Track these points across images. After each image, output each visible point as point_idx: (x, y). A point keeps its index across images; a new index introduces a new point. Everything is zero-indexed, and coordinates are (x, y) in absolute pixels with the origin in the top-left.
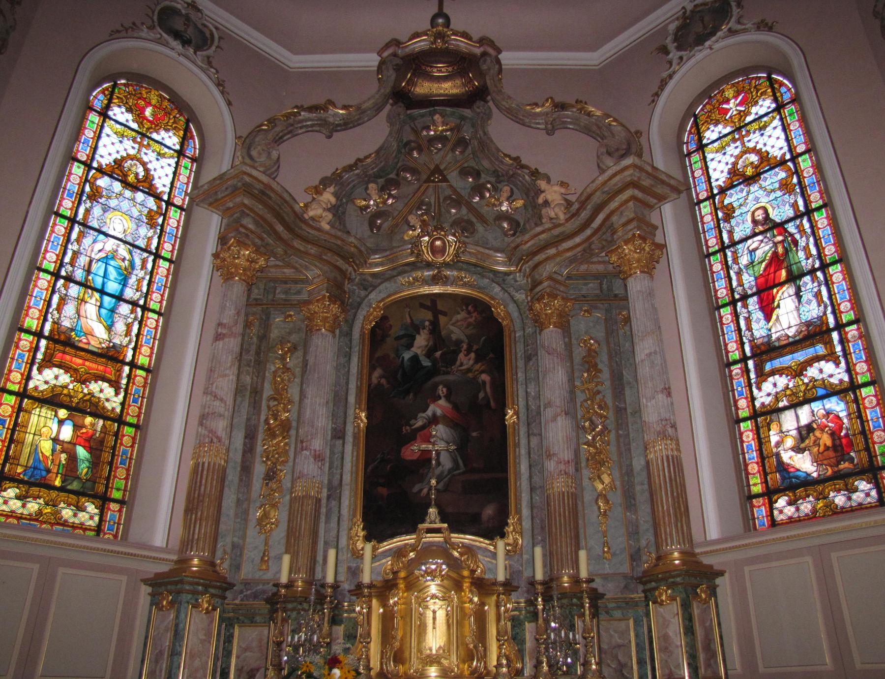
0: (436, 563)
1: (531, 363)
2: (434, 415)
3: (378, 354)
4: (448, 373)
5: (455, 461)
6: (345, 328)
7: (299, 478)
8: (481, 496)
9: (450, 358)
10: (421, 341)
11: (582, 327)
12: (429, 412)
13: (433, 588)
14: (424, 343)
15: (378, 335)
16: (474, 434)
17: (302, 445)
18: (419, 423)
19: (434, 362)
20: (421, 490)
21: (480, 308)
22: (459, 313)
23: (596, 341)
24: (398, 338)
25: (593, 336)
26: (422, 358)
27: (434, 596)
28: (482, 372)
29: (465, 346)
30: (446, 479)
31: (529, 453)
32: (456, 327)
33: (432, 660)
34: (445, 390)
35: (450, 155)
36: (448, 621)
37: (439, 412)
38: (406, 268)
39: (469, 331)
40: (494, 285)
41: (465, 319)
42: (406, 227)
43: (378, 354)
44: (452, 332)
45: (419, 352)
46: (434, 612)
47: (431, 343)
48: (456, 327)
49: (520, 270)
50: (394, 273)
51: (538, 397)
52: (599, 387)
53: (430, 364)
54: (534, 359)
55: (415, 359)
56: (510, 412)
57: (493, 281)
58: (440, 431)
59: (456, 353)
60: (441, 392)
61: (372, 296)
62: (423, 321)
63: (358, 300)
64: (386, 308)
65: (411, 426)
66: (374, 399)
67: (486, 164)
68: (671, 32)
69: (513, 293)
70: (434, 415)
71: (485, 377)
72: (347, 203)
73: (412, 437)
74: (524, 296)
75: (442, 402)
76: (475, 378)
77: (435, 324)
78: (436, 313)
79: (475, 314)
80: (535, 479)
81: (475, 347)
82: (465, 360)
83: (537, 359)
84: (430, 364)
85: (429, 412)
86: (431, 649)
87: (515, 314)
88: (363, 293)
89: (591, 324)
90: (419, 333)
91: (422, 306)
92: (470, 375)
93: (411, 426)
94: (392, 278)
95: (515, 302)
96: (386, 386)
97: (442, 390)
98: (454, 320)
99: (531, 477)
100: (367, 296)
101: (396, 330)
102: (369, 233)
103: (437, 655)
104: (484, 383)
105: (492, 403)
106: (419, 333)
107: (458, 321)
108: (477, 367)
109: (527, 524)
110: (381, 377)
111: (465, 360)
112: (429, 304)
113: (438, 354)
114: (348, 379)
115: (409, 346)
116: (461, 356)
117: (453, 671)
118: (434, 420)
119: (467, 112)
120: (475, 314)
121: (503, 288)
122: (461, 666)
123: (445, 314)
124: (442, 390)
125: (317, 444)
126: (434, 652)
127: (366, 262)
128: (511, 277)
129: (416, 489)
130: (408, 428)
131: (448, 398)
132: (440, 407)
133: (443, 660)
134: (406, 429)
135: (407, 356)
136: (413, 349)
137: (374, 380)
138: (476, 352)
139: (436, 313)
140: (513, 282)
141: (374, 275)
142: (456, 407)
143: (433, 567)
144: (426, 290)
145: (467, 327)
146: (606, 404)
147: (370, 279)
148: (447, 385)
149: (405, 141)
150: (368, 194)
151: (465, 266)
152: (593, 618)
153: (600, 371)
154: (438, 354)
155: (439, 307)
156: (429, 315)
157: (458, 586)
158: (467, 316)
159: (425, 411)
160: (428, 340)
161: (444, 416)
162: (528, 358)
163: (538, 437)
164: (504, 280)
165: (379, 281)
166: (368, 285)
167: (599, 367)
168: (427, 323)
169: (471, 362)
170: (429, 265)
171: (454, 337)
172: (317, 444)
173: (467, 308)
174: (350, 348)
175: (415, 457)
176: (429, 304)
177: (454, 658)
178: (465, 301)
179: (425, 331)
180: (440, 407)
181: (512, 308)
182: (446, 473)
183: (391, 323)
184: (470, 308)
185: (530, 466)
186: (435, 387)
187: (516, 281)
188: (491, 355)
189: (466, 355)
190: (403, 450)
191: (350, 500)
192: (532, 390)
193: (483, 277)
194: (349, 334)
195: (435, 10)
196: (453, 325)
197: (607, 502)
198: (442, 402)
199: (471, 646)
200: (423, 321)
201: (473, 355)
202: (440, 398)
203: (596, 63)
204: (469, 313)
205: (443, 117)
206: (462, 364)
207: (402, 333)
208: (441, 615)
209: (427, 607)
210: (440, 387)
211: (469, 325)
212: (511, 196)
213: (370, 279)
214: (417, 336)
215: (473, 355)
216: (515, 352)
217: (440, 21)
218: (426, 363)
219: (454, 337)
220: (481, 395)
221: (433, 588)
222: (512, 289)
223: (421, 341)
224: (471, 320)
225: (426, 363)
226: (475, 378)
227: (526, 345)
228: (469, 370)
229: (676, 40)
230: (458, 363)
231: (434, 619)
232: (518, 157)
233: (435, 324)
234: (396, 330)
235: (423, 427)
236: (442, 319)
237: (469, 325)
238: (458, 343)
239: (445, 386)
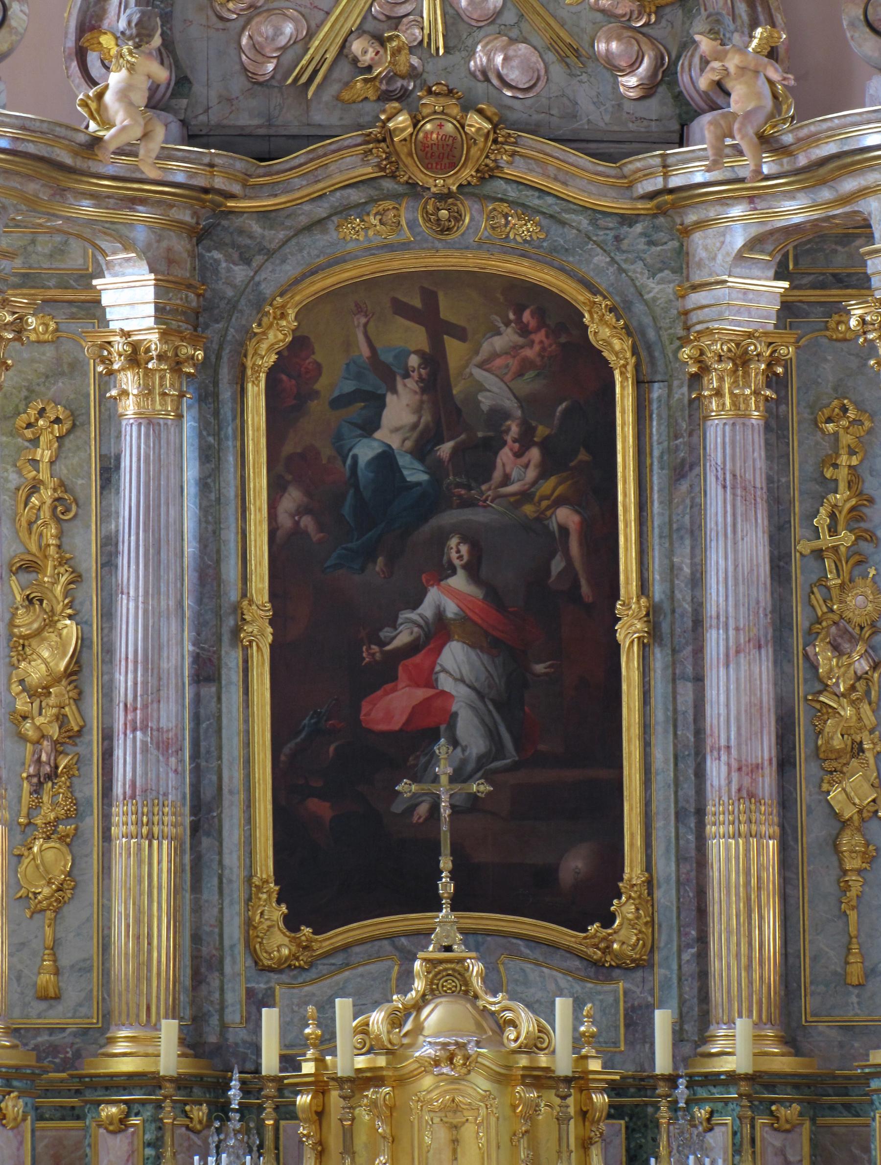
2: (440, 615)
3: (288, 448)
5: (492, 735)
9: (478, 458)
10: (400, 411)
12: (427, 609)
16: (540, 668)
18: (403, 638)
19: (436, 470)
22: (499, 333)
28: (559, 502)
29: (514, 429)
34: (464, 549)
37: (451, 609)
43: (288, 448)
44: (482, 388)
45: (395, 442)
47: (426, 418)
48: (491, 370)
55: (386, 458)
58: (455, 656)
59: (493, 445)
60: (454, 555)
62: (403, 355)
65: (382, 644)
70: (440, 615)
71: (565, 516)
73: (385, 673)
75: (459, 582)
76: (541, 519)
78: (438, 329)
79: (540, 336)
81: (542, 431)
82: (517, 468)
91: (402, 309)
92: (529, 509)
93: (382, 644)
96: (315, 536)
97: (457, 550)
101: (332, 380)
104: (564, 530)
105: (585, 589)
108: (547, 486)
110: (301, 511)
111: (517, 468)
112: (417, 303)
113: (445, 449)
115: (370, 426)
116: (505, 455)
118: (438, 632)
123: (461, 334)
124: (457, 550)
130: (375, 648)
131: (473, 570)
132: (453, 593)
134: (370, 653)
135: (365, 452)
137: (285, 521)
138: (545, 446)
139: (438, 329)
142: (493, 594)
145: (520, 374)
154: (445, 449)
155: (447, 311)
160: (418, 410)
161: (464, 620)
168: (414, 361)
169: (531, 474)
175: (396, 724)
176: (417, 303)
179: (411, 383)
180: (453, 593)
186: (440, 540)
188: (583, 456)
190: (365, 707)
198: (459, 582)
201: (535, 454)
204: (524, 331)
206: (506, 480)
207: (349, 386)
210: (453, 542)
211: (525, 366)
213: (256, 228)
214: (390, 398)
218: (415, 473)
219: (486, 401)
220: (557, 565)
223: (400, 411)
224: (529, 353)
226: (541, 519)
228: (525, 496)
230: (497, 475)
234: (332, 380)
235: (413, 648)
237: (525, 366)
238: (498, 416)
239: (464, 539)
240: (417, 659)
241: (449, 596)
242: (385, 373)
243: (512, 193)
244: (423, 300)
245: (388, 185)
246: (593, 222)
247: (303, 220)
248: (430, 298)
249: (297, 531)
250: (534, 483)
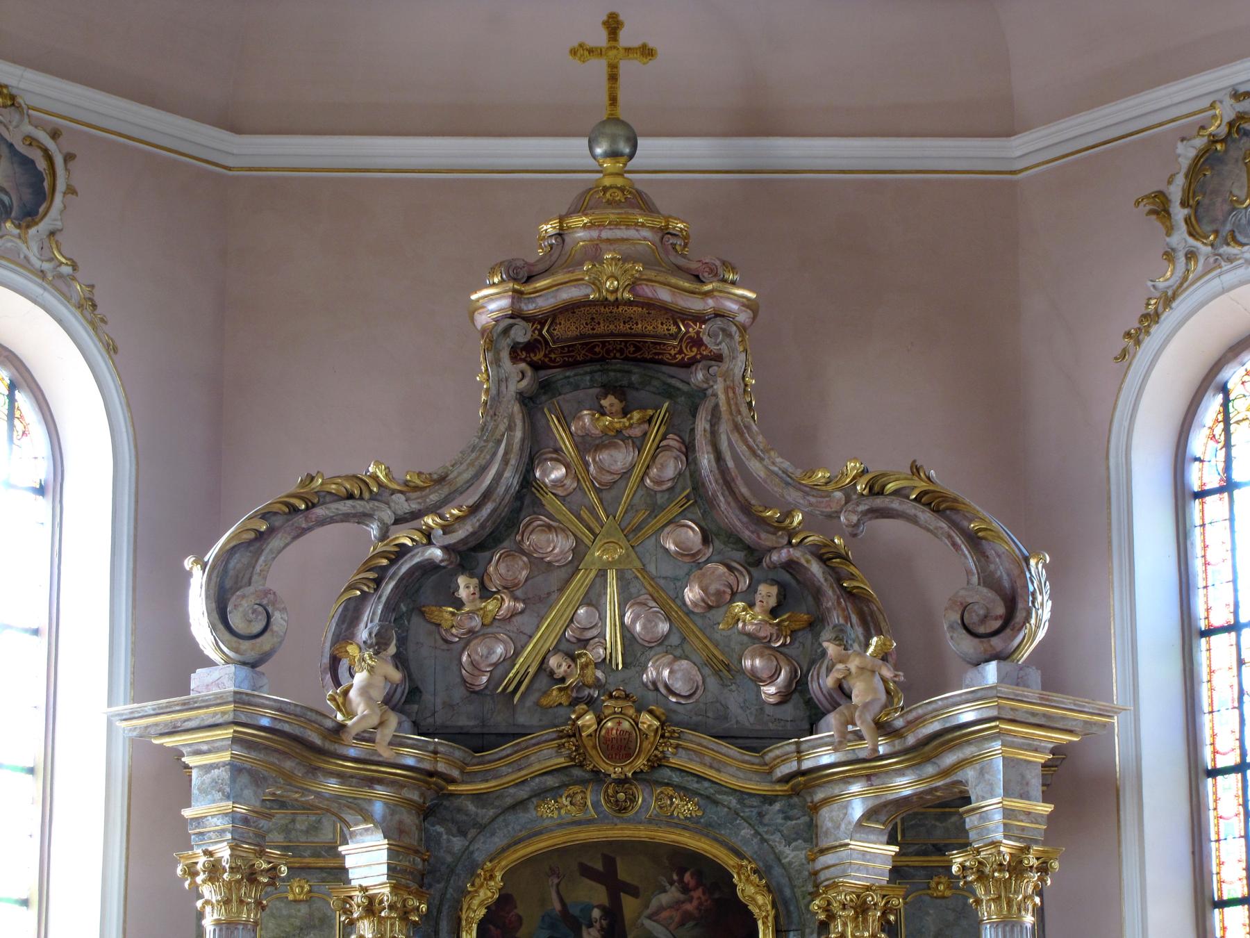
22: (665, 891)
38: (551, 781)
41: (676, 904)
62: (588, 909)
78: (617, 889)
79: (698, 893)
91: (587, 872)
98: (654, 903)
107: (661, 908)
112: (599, 866)
120: (698, 893)
123: (634, 892)
128: (777, 806)
139: (617, 889)
145: (682, 924)
151: (676, 778)
155: (623, 874)
156: (597, 894)
158: (682, 897)
164: (761, 815)
165: (491, 812)
168: (596, 913)
173: (681, 872)
176: (599, 866)
183: (520, 910)
184: (687, 877)
196: (650, 917)
200: (588, 909)
204: (685, 889)
211: (686, 917)
213: (471, 808)
222: (777, 837)
224: (688, 907)
236: (629, 904)
243: (676, 778)
244: (603, 865)
245: (577, 772)
246: (741, 801)
247: (509, 801)
248: (610, 862)
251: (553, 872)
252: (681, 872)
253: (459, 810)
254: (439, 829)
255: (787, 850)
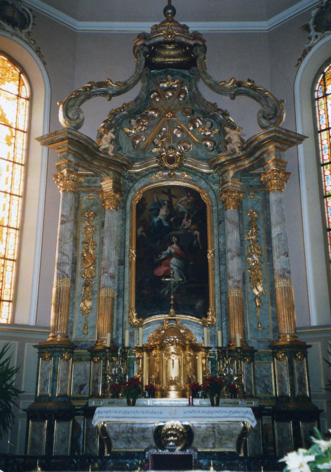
0: (174, 338)
1: (221, 226)
2: (171, 252)
3: (140, 219)
4: (177, 230)
6: (122, 204)
7: (103, 288)
8: (194, 296)
9: (179, 221)
10: (163, 212)
11: (250, 204)
12: (168, 251)
13: (172, 349)
14: (164, 213)
15: (141, 207)
16: (191, 263)
17: (105, 270)
18: (163, 257)
19: (170, 223)
20: (164, 293)
21: (194, 194)
22: (183, 197)
23: (257, 213)
24: (151, 210)
25: (255, 209)
26: (163, 221)
27: (173, 353)
28: (195, 230)
30: (177, 286)
31: (220, 274)
32: (181, 204)
33: (172, 383)
34: (176, 239)
35: (177, 100)
36: (179, 365)
37: (173, 251)
38: (154, 170)
39: (188, 207)
40: (202, 179)
41: (186, 200)
42: (153, 145)
43: (140, 219)
44: (179, 207)
45: (162, 218)
46: (173, 360)
48: (181, 204)
49: (216, 172)
50: (147, 173)
51: (225, 244)
52: (258, 239)
53: (168, 225)
54: (223, 223)
55: (160, 221)
56: (210, 251)
57: (201, 178)
58: (174, 261)
61: (136, 185)
62: (164, 201)
63: (129, 188)
64: (144, 193)
65: (158, 258)
66: (140, 244)
67: (197, 106)
68: (313, 15)
69: (212, 185)
70: (171, 252)
71: (196, 232)
72: (119, 129)
73: (160, 263)
74: (217, 187)
75: (174, 246)
77: (170, 203)
78: (171, 196)
80: (223, 288)
81: (192, 216)
82: (187, 223)
83: (224, 224)
84: (168, 225)
85: (168, 251)
86: (172, 378)
87: (213, 197)
88: (131, 184)
89: (255, 203)
90: (162, 208)
91: (163, 192)
92: (189, 231)
93: (158, 258)
94: (146, 176)
95: (213, 190)
97: (174, 239)
98: (180, 200)
99: (220, 287)
100: (133, 186)
101: (150, 206)
102: (133, 148)
103: (175, 381)
104: (196, 235)
106: (162, 208)
107: (182, 201)
108: (193, 227)
109: (218, 311)
110: (142, 232)
111: (187, 223)
113: (172, 219)
114: (125, 233)
115: (157, 215)
116: (184, 221)
117: (182, 388)
119: (187, 72)
120: (191, 197)
121: (206, 182)
122: (186, 385)
123: (175, 197)
124: (174, 239)
125: (112, 270)
126: (173, 379)
127: (132, 167)
128: (211, 176)
129: (162, 291)
131: (178, 243)
132: (174, 248)
133: (177, 383)
135: (156, 220)
136: (159, 216)
137: (139, 233)
139: (171, 196)
140: (211, 178)
141: (137, 174)
143: (172, 339)
144: (165, 183)
145: (187, 205)
146: (261, 248)
147: (134, 176)
148: (177, 236)
149: (151, 90)
150: (132, 126)
151: (186, 169)
152: (251, 362)
153: (258, 230)
154: (172, 219)
155: (173, 192)
156: (167, 198)
157: (184, 348)
158: (187, 198)
159: (166, 250)
160: (167, 212)
162: (220, 223)
163: (224, 266)
164: (207, 178)
165: (139, 177)
166: (133, 179)
167: (258, 227)
168: (166, 202)
169: (190, 224)
170: (166, 169)
171: (180, 210)
172: (112, 270)
173: (187, 193)
174: (125, 215)
176: (166, 191)
177: (182, 382)
178: (187, 190)
179: (165, 207)
180: (174, 248)
181: (211, 193)
182: (177, 283)
183: (147, 201)
184: (189, 194)
185: (220, 281)
187: (214, 178)
189: (187, 220)
191: (130, 297)
192: (221, 240)
193: (195, 175)
194: (124, 208)
195: (166, 4)
196: (179, 203)
197: (260, 301)
198: (174, 246)
199: (190, 376)
200: (164, 201)
201: (190, 220)
202: (173, 243)
203: (267, 28)
204: (188, 197)
205: (172, 76)
206: (185, 225)
207: (153, 207)
208: (176, 362)
209: (170, 358)
211: (188, 203)
212: (211, 127)
213: (134, 176)
214: (161, 209)
215: (190, 220)
216: (211, 219)
217: (170, 11)
218: (166, 224)
219: (180, 210)
220: (195, 242)
221: (172, 349)
222: (211, 183)
223: (163, 212)
224: (189, 201)
225: (166, 224)
227: (219, 215)
228: (188, 229)
229: (315, 23)
230: (183, 224)
231: (173, 363)
232: (215, 104)
233: (170, 203)
234: (150, 206)
236: (174, 200)
237: (188, 203)
238: (183, 213)
239: (176, 237)
240: (166, 261)
241: (173, 248)
242: (160, 205)
245: (161, 168)
247: (144, 174)
249: (141, 236)
250: (190, 226)
251: (155, 192)
252: (187, 193)
253: (131, 177)
254: (126, 181)
255: (214, 186)
